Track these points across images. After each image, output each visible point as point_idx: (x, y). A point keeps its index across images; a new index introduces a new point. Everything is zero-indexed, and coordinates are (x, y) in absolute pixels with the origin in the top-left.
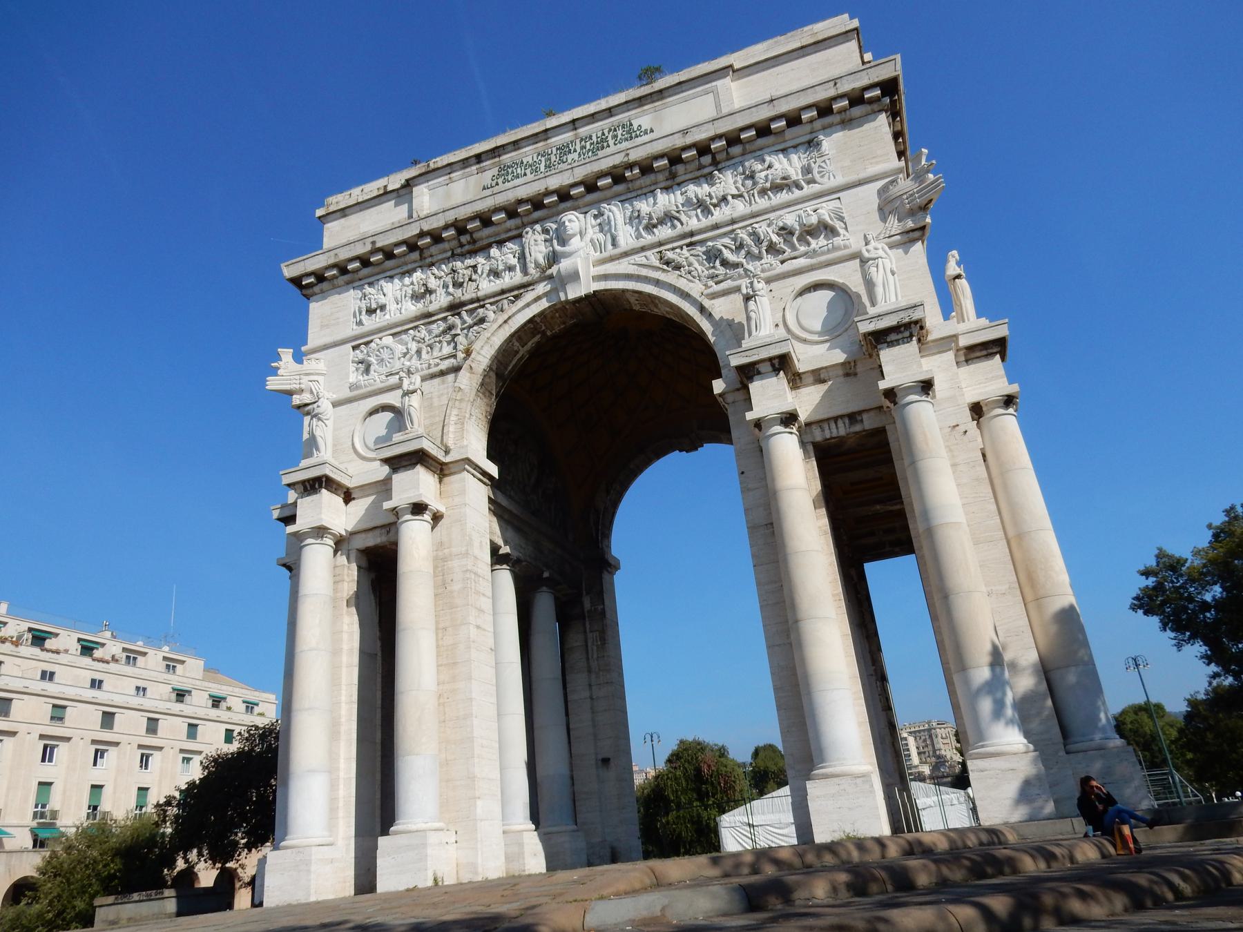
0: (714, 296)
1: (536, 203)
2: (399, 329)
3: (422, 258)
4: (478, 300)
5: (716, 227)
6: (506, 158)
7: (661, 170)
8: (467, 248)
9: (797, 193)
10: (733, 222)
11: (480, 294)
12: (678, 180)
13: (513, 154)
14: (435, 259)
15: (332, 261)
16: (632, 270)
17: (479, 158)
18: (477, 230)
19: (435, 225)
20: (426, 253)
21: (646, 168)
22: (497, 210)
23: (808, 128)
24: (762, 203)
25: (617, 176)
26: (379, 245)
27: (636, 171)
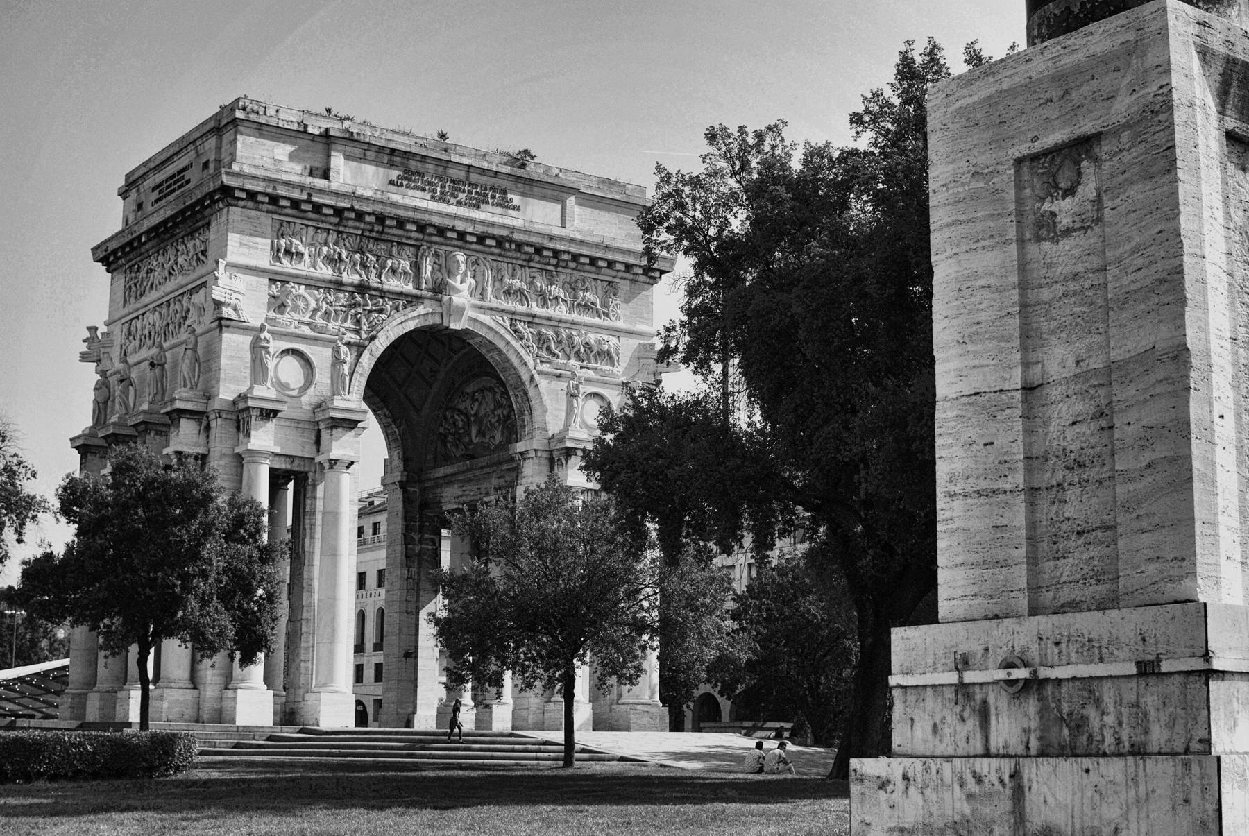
0: (540, 373)
1: (442, 231)
2: (312, 283)
3: (338, 224)
4: (381, 291)
5: (550, 319)
6: (413, 164)
7: (526, 253)
8: (374, 235)
9: (597, 321)
10: (560, 321)
11: (386, 287)
12: (532, 264)
13: (419, 164)
14: (347, 230)
15: (270, 191)
16: (493, 325)
17: (393, 150)
18: (391, 227)
19: (364, 208)
20: (344, 222)
21: (519, 246)
22: (414, 222)
23: (614, 273)
24: (575, 316)
25: (500, 241)
26: (314, 199)
27: (513, 246)
